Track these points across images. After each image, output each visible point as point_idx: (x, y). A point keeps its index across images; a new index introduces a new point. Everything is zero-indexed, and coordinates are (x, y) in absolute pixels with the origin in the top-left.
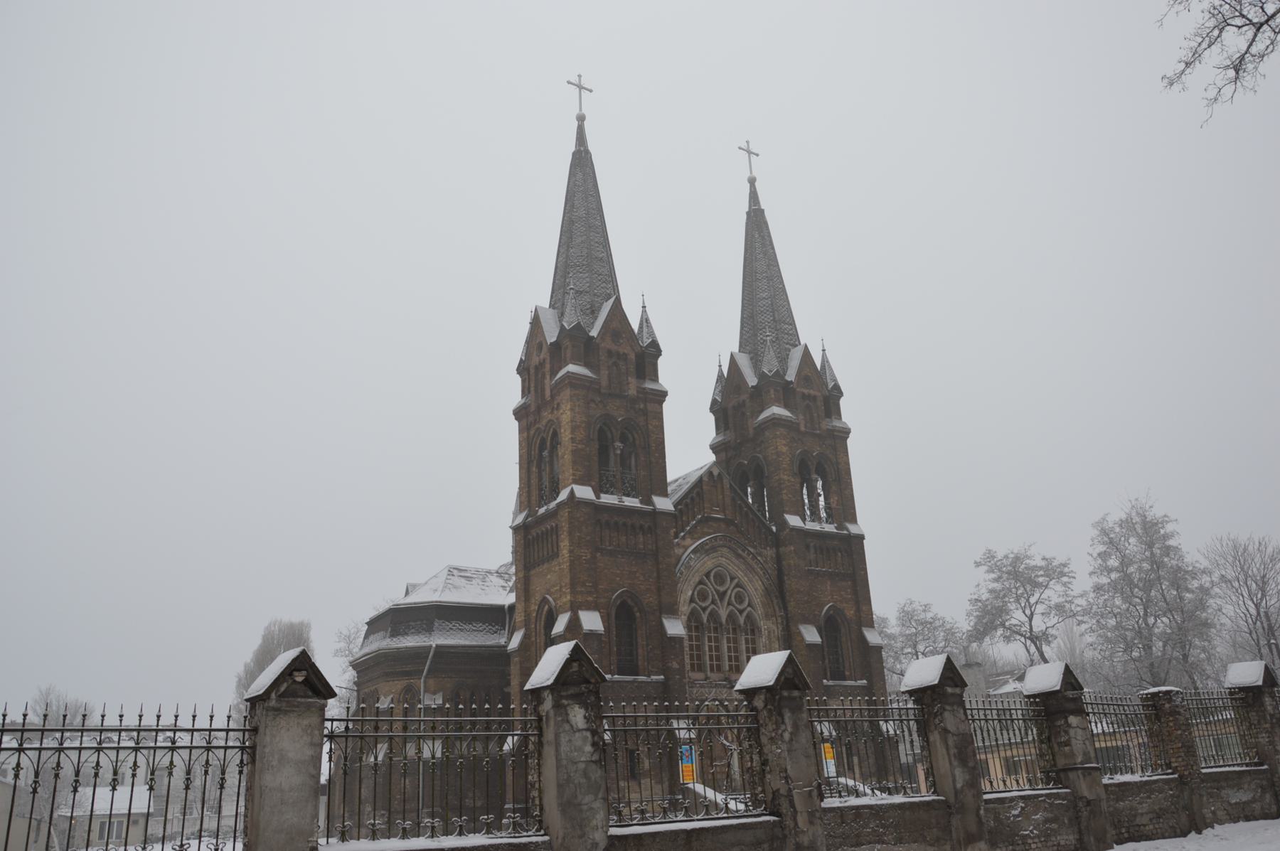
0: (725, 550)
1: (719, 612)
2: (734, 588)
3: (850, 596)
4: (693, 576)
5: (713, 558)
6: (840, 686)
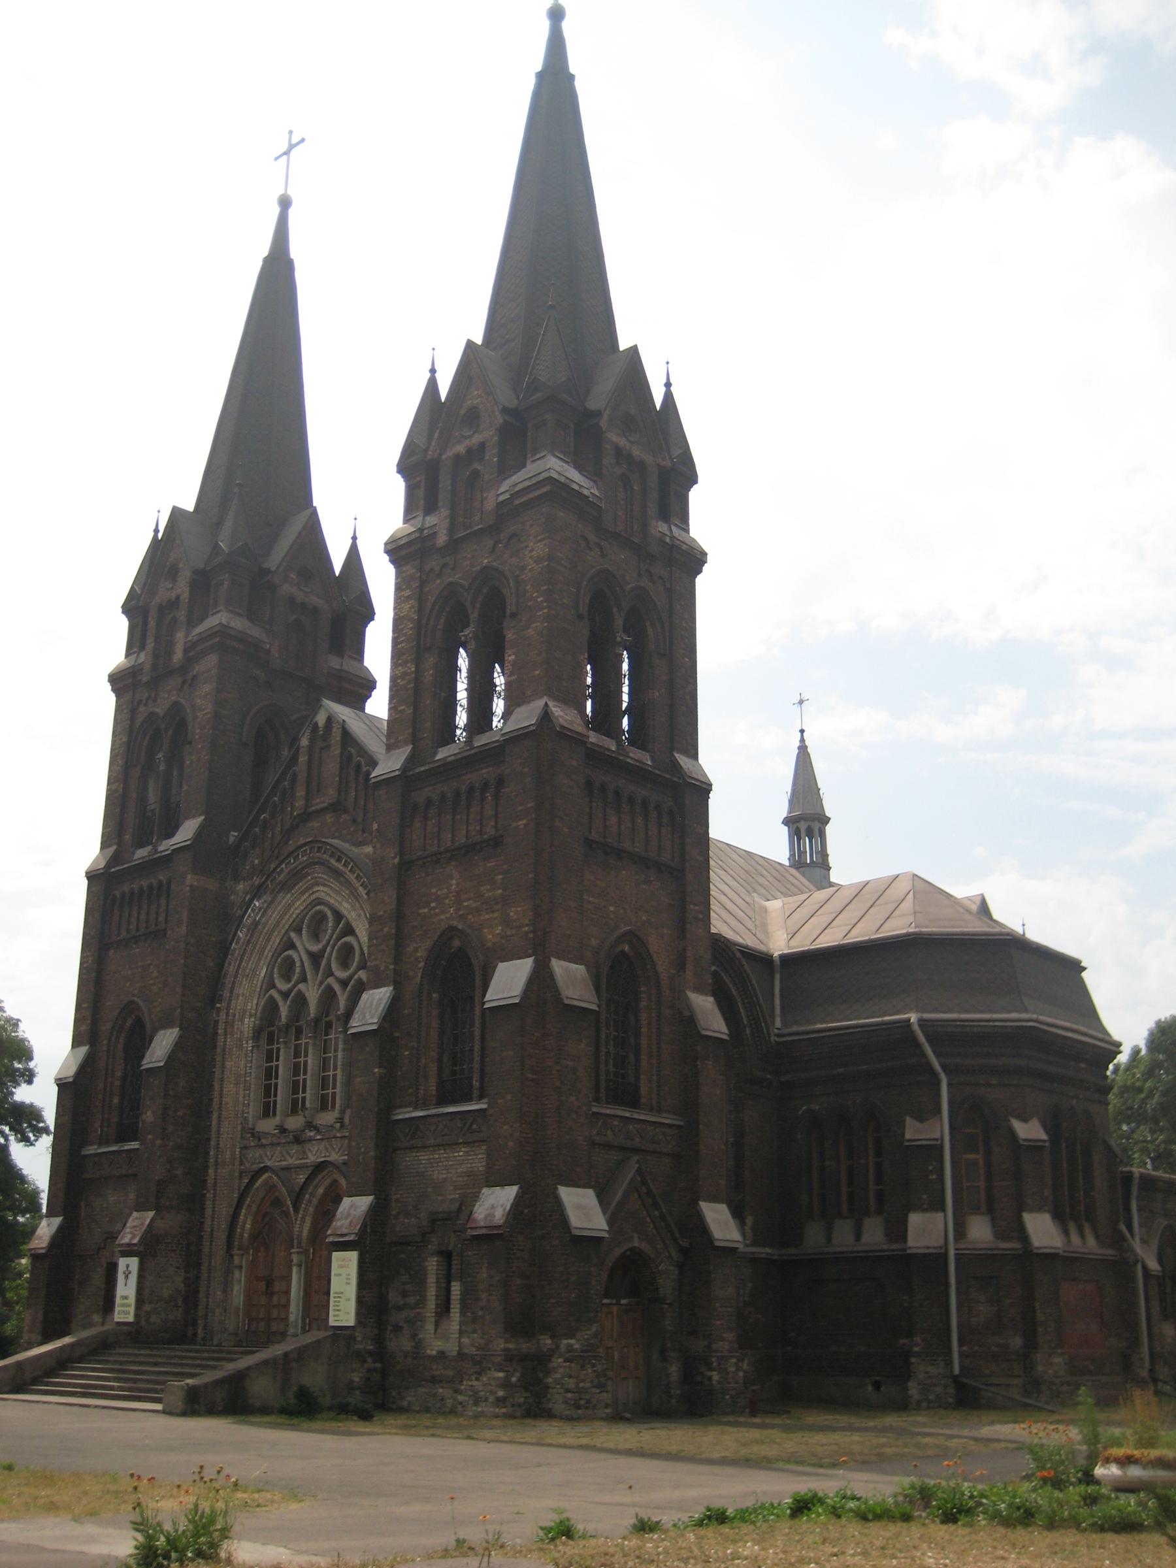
0: (319, 873)
1: (307, 995)
2: (339, 939)
3: (500, 891)
4: (268, 940)
5: (303, 893)
6: (439, 1115)
